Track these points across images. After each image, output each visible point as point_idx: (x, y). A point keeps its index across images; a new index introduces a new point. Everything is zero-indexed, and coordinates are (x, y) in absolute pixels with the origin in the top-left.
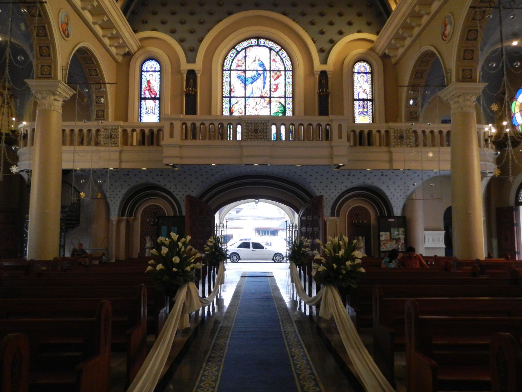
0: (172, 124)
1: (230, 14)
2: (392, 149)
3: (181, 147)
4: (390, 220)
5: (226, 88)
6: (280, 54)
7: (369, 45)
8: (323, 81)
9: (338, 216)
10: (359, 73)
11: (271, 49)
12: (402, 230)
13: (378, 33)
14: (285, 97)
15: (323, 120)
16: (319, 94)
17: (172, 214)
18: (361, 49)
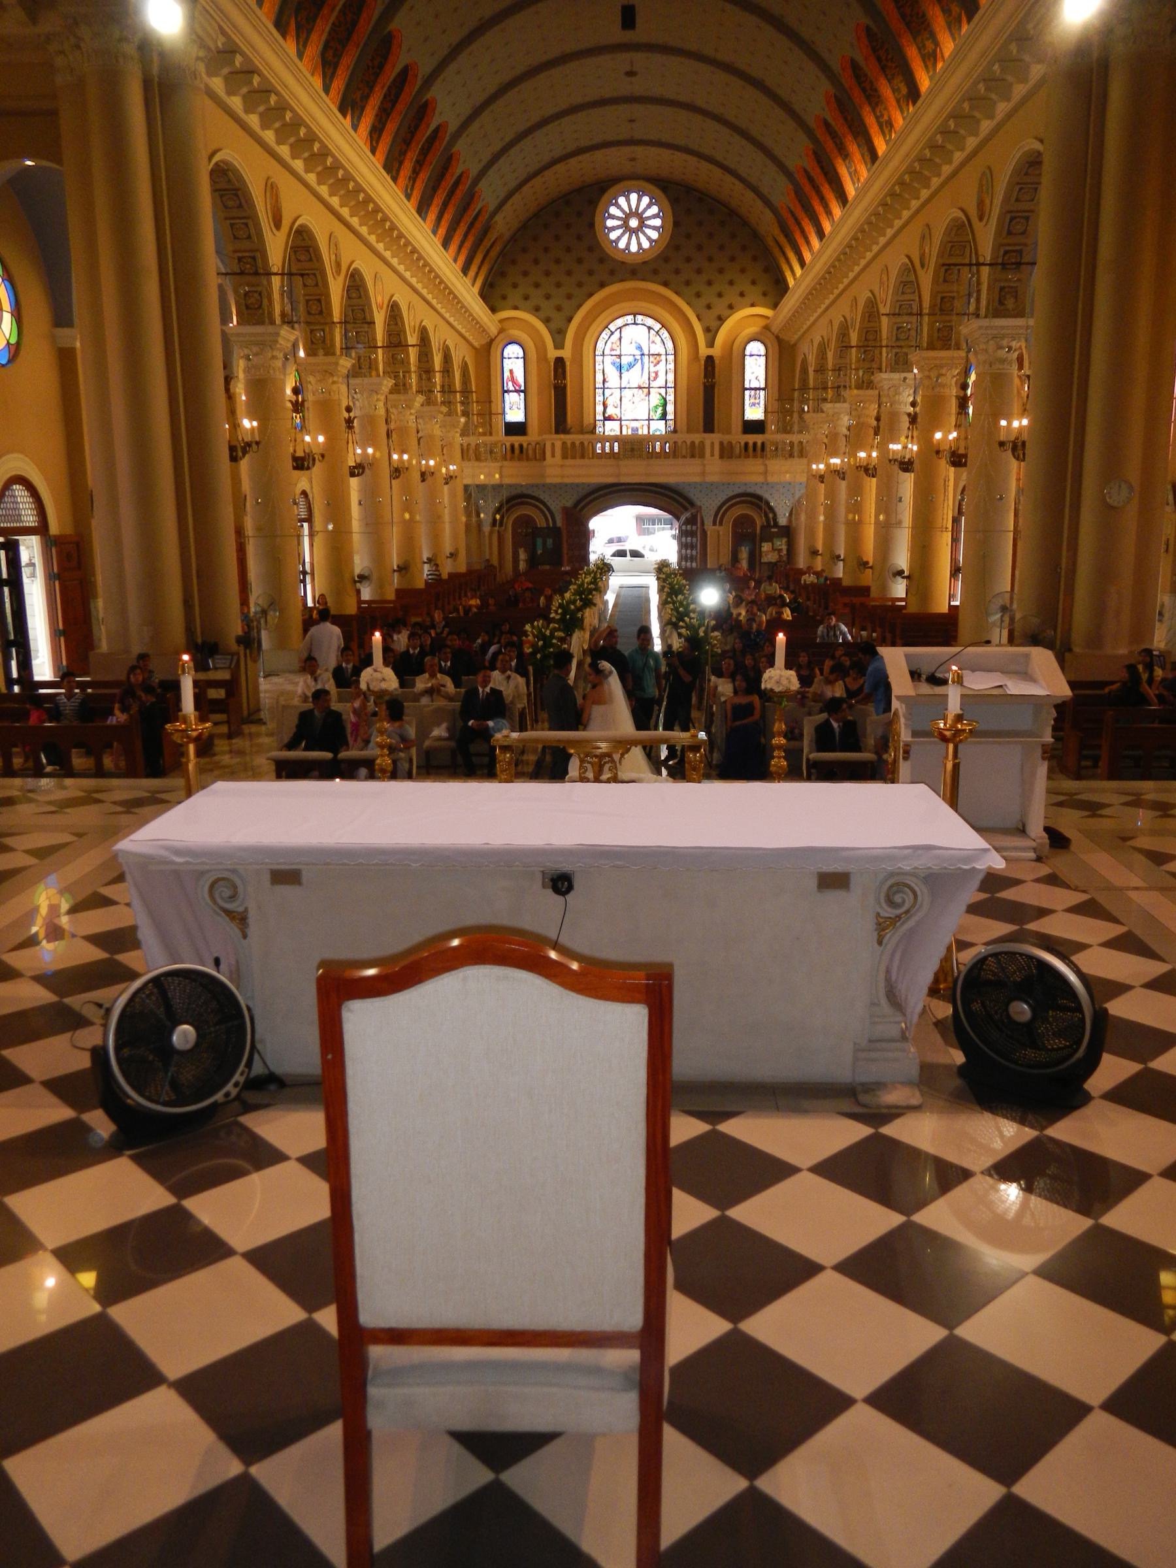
0: (553, 444)
1: (602, 285)
2: (767, 462)
3: (562, 466)
4: (773, 530)
5: (599, 378)
6: (660, 333)
7: (763, 322)
8: (710, 368)
9: (721, 524)
10: (751, 355)
11: (649, 328)
12: (784, 540)
13: (775, 306)
14: (666, 387)
15: (697, 438)
16: (704, 383)
17: (545, 525)
18: (752, 330)
